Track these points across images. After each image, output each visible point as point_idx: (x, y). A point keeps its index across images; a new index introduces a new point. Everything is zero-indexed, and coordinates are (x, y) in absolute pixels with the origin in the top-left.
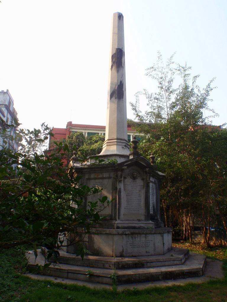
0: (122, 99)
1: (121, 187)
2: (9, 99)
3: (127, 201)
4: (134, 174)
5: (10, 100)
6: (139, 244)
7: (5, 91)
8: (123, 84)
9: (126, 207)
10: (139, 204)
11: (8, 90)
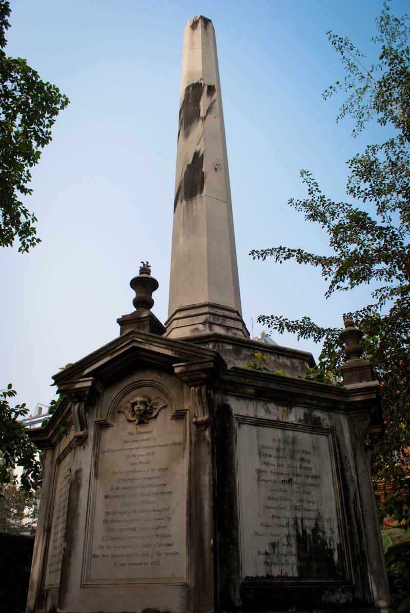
0: (198, 196)
1: (82, 466)
3: (105, 521)
4: (135, 404)
8: (202, 155)
10: (160, 531)
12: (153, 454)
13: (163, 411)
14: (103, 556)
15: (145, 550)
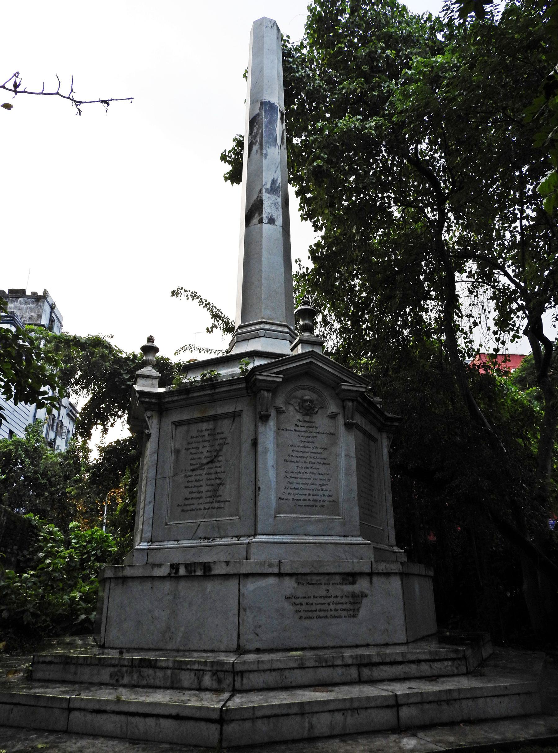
2: (51, 313)
3: (286, 477)
5: (53, 315)
6: (324, 607)
7: (40, 293)
9: (282, 497)
10: (324, 487)
11: (45, 292)
12: (316, 437)
13: (320, 410)
14: (286, 499)
15: (315, 498)
